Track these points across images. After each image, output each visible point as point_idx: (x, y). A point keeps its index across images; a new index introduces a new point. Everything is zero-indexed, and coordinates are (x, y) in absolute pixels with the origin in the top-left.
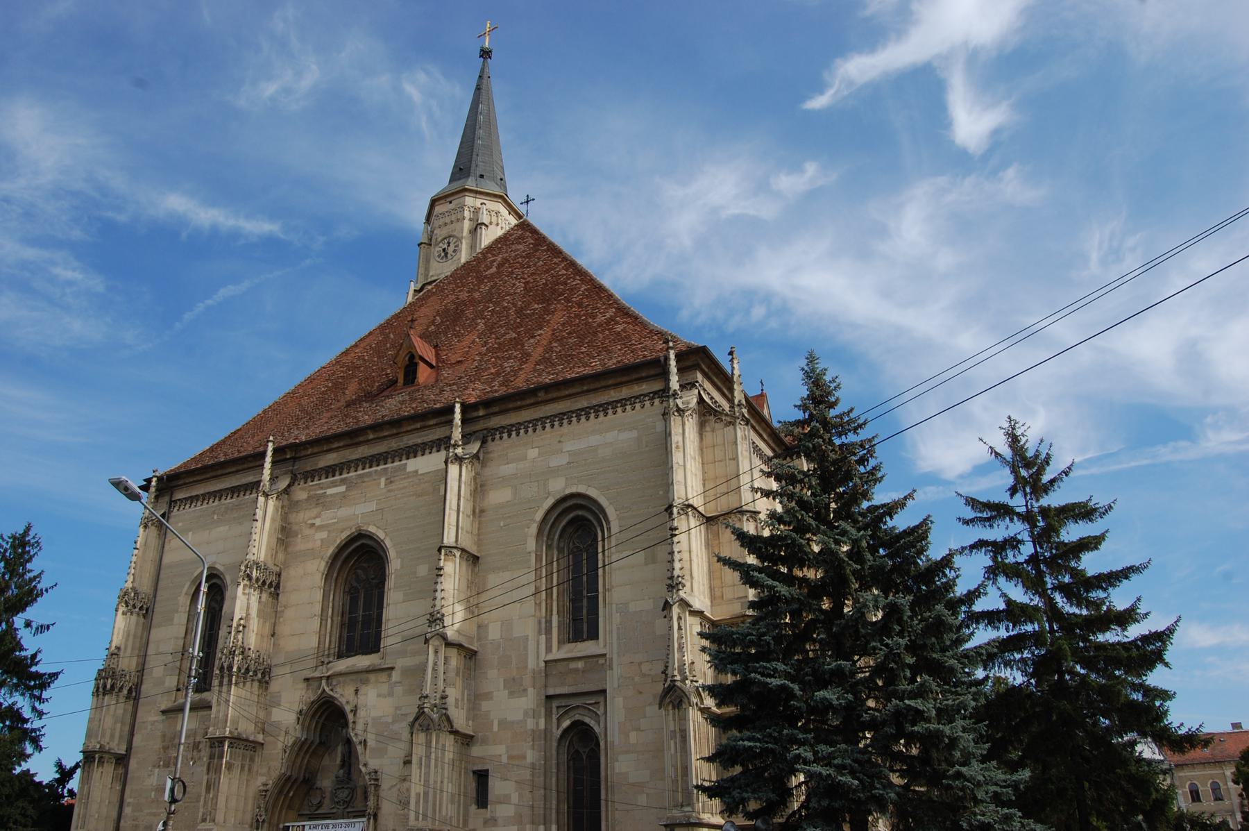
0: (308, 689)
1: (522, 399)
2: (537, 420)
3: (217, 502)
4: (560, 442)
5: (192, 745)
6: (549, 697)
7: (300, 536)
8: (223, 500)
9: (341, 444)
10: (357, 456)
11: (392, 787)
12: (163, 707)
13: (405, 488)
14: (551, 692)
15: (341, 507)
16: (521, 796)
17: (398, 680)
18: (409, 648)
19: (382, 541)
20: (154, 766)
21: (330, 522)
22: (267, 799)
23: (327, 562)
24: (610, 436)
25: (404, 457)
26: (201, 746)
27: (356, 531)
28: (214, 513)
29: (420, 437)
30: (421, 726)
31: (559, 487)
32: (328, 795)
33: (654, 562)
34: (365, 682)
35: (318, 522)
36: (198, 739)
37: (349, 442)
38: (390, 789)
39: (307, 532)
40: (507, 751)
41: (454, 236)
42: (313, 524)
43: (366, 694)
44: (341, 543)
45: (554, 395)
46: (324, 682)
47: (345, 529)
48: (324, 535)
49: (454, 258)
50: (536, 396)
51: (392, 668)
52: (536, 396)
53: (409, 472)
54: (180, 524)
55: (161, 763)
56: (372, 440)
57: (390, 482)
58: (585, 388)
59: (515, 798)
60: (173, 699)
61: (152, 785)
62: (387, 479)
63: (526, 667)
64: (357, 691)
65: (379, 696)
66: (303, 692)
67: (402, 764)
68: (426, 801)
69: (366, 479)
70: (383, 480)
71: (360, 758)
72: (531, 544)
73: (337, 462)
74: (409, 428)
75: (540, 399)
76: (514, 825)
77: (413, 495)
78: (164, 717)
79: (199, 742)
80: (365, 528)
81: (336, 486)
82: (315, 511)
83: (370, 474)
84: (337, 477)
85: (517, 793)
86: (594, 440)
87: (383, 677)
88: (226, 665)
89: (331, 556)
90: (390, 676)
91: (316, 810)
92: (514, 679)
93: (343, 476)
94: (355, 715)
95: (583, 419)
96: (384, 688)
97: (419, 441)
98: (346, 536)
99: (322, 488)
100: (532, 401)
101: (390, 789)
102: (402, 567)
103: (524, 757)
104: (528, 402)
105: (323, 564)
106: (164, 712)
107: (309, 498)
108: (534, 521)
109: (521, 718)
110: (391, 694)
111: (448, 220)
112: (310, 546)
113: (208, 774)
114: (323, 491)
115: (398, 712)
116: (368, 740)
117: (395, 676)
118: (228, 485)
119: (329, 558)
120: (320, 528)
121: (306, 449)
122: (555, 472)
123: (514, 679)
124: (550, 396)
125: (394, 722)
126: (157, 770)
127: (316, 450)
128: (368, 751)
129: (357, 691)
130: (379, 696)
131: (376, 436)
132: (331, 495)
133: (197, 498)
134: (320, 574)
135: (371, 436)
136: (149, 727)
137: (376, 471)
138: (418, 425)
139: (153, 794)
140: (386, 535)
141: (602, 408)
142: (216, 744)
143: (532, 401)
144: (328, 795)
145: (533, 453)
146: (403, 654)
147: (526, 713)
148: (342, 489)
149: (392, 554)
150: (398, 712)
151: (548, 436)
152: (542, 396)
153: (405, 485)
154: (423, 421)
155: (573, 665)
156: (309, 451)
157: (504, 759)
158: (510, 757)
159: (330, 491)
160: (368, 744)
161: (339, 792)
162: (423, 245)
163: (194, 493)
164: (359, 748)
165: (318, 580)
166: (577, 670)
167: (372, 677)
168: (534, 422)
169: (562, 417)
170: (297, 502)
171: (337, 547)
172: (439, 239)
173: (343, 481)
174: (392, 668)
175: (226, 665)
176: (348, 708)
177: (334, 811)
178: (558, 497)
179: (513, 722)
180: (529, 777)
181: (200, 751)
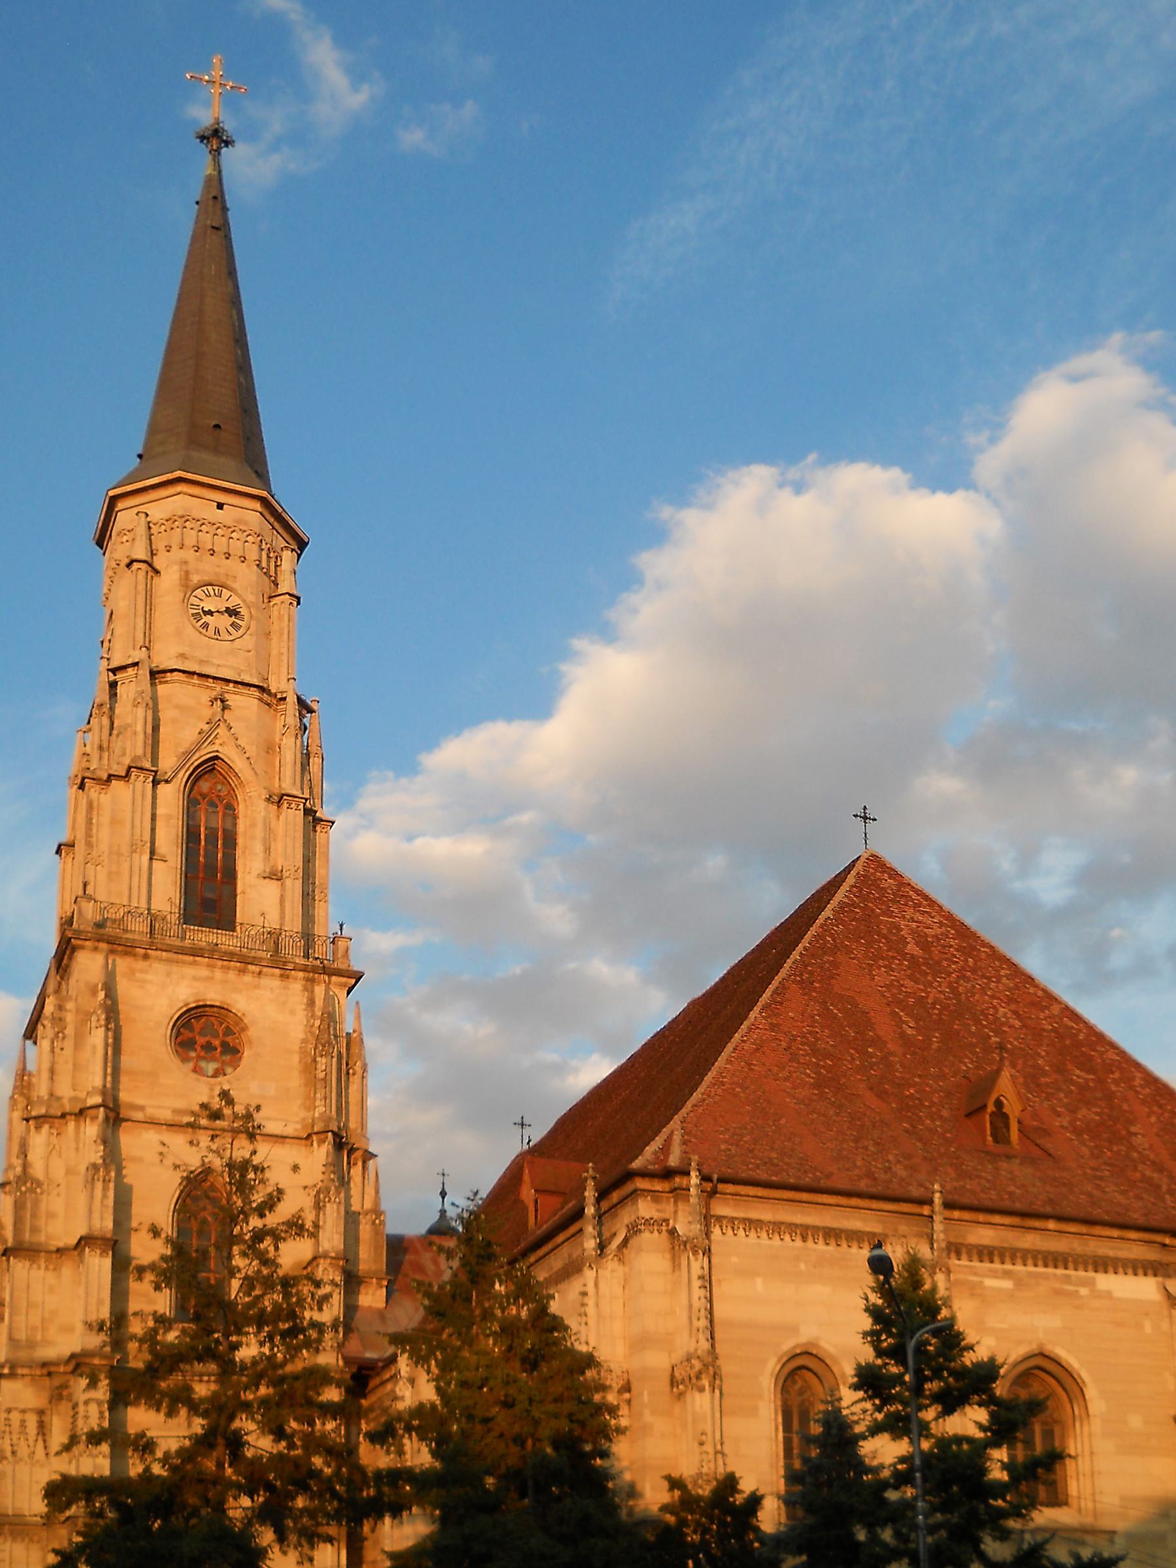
8: (810, 1243)
29: (1112, 1248)
54: (734, 1259)
73: (995, 1243)
81: (996, 1277)
97: (1111, 1253)
99: (975, 1274)
111: (221, 544)
127: (967, 1215)
137: (1055, 1275)
148: (1007, 1284)
149: (1091, 1392)
159: (990, 1282)
163: (754, 1215)
172: (195, 579)
173: (1007, 1274)
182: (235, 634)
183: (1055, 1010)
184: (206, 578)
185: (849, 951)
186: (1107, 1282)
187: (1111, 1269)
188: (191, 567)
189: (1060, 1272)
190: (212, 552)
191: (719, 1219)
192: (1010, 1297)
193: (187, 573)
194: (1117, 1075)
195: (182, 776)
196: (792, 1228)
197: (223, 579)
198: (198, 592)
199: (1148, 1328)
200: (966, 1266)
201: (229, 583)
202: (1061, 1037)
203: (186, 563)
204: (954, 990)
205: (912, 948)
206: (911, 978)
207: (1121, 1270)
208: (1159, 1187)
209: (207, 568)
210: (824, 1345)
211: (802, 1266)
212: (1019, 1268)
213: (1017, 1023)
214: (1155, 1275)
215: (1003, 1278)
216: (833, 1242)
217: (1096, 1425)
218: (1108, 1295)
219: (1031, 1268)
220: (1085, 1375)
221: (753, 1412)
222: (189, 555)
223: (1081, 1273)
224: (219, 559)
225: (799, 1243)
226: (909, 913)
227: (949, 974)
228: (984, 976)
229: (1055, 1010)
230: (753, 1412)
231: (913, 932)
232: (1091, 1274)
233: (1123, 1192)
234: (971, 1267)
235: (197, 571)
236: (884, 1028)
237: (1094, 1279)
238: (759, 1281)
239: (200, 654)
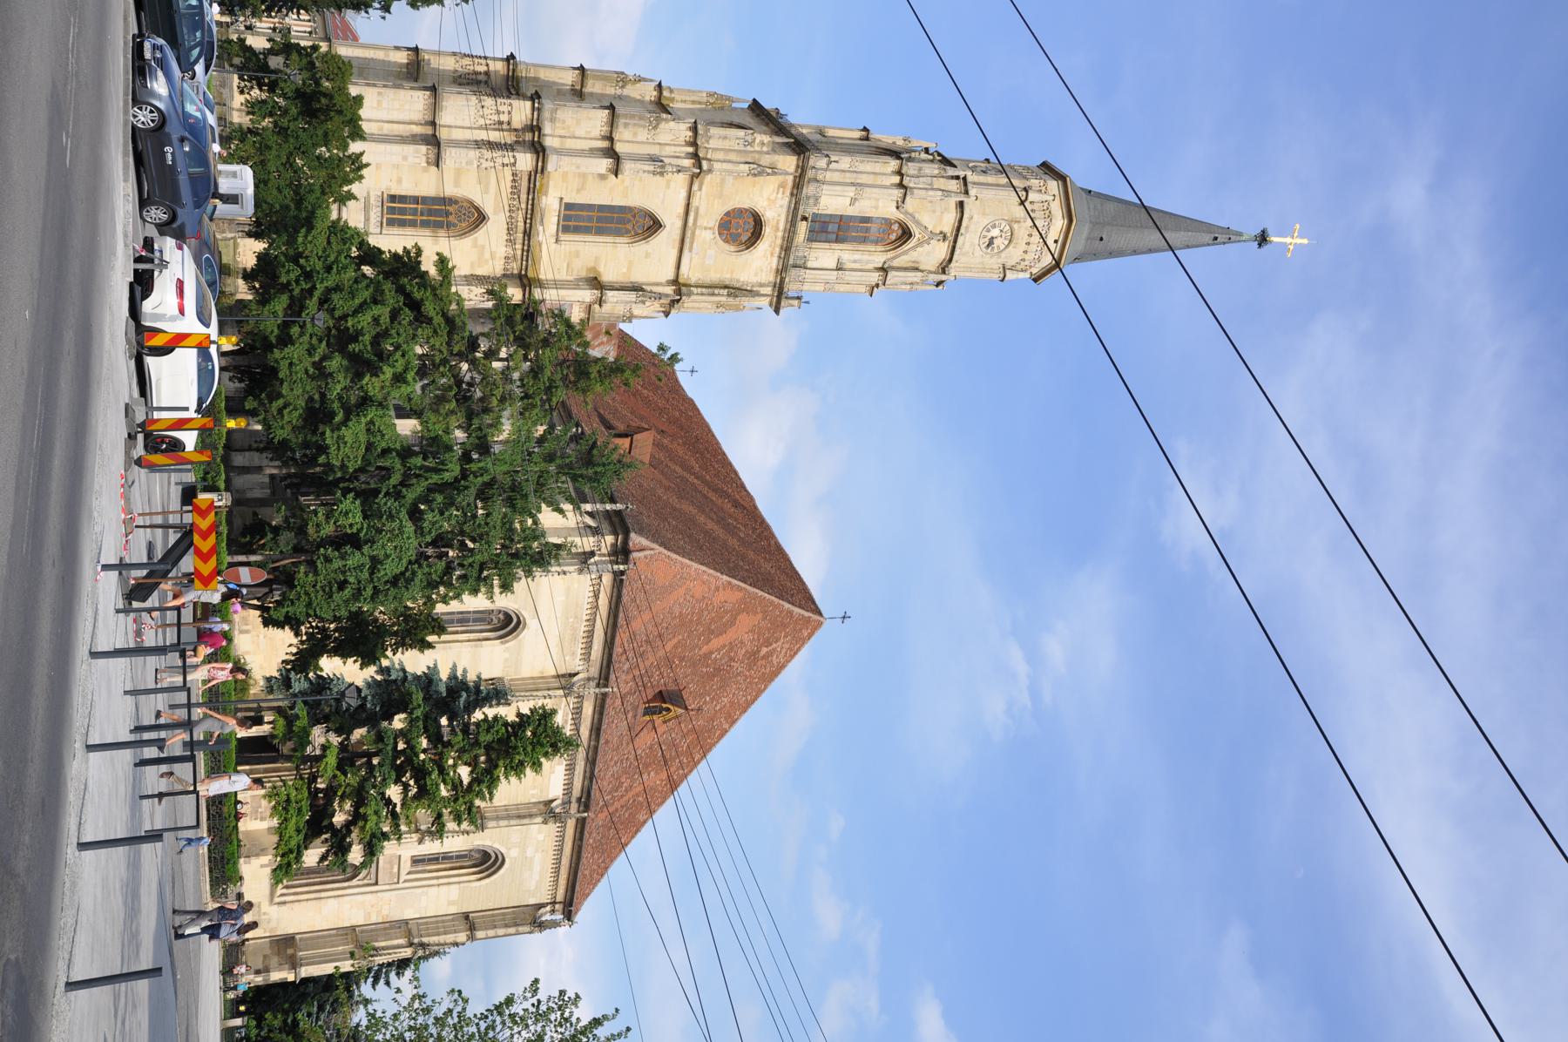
24: (536, 877)
31: (511, 855)
33: (449, 905)
41: (1007, 246)
73: (583, 716)
86: (537, 867)
97: (576, 773)
133: (596, 596)
141: (557, 871)
155: (396, 867)
166: (392, 868)
169: (560, 850)
172: (1016, 226)
183: (726, 726)
184: (1016, 232)
185: (764, 618)
188: (1022, 224)
193: (1019, 222)
194: (685, 761)
195: (901, 217)
198: (1008, 227)
199: (535, 792)
201: (1012, 245)
202: (710, 731)
204: (738, 674)
205: (764, 650)
206: (747, 651)
208: (616, 791)
210: (526, 630)
211: (571, 620)
213: (718, 708)
216: (585, 635)
224: (1026, 239)
226: (787, 646)
227: (749, 670)
228: (747, 688)
229: (726, 726)
231: (774, 650)
233: (613, 775)
236: (715, 643)
238: (564, 598)
239: (972, 227)
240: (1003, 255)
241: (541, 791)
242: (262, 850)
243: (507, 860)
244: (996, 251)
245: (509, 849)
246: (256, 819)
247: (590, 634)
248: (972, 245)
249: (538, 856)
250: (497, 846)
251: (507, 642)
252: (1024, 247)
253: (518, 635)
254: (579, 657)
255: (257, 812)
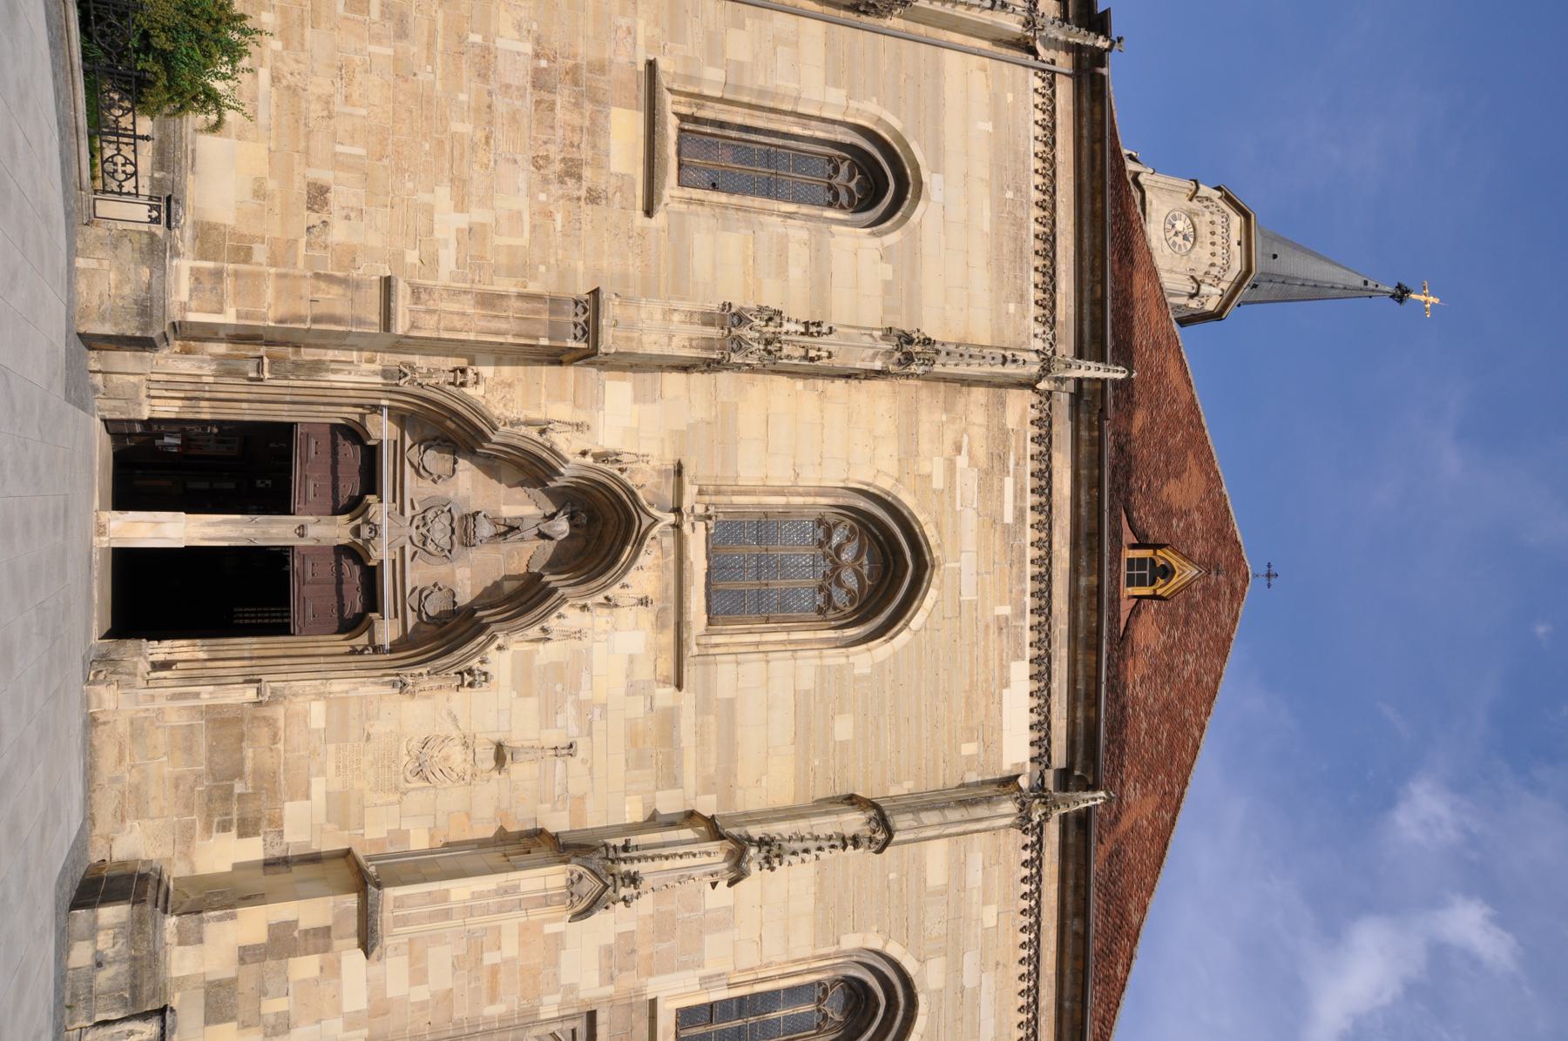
0: (660, 472)
1: (1077, 887)
2: (1038, 916)
3: (1036, 196)
4: (998, 964)
5: (576, 156)
6: (591, 1017)
7: (944, 418)
8: (1037, 212)
9: (1083, 512)
10: (1055, 546)
11: (455, 719)
12: (663, 64)
13: (986, 661)
14: (601, 1018)
15: (979, 515)
16: (423, 1006)
17: (658, 704)
18: (711, 718)
19: (906, 625)
20: (538, 41)
21: (958, 492)
22: (448, 387)
23: (888, 493)
25: (1036, 652)
26: (571, 182)
27: (932, 559)
28: (1018, 190)
30: (580, 877)
31: (929, 978)
32: (441, 489)
34: (660, 625)
35: (962, 461)
36: (587, 173)
37: (1084, 529)
38: (450, 714)
39: (949, 437)
40: (506, 962)
41: (1194, 245)
42: (958, 450)
43: (637, 627)
44: (917, 522)
45: (1069, 950)
46: (671, 518)
47: (938, 526)
48: (938, 482)
49: (1164, 242)
50: (1076, 915)
51: (679, 686)
52: (1076, 915)
53: (1008, 667)
54: (1010, 97)
55: (543, 63)
56: (1077, 580)
57: (1002, 625)
58: (1067, 1004)
59: (421, 993)
60: (675, 87)
61: (497, 34)
62: (1007, 618)
63: (651, 974)
64: (644, 602)
65: (632, 659)
66: (655, 463)
67: (497, 737)
68: (433, 917)
69: (1015, 570)
70: (1005, 610)
71: (517, 636)
72: (851, 942)
73: (1055, 497)
74: (1080, 666)
75: (1068, 922)
76: (369, 1001)
77: (971, 683)
78: (641, 67)
79: (580, 178)
80: (935, 580)
82: (981, 453)
83: (1021, 580)
84: (1031, 499)
85: (427, 996)
87: (667, 666)
88: (745, 332)
89: (899, 501)
90: (665, 682)
91: (412, 464)
92: (633, 951)
93: (1029, 510)
94: (601, 605)
95: (1022, 1001)
96: (644, 672)
97: (1054, 685)
98: (928, 533)
99: (1017, 464)
100: (1070, 908)
101: (450, 714)
102: (856, 679)
103: (493, 1000)
104: (1070, 899)
105: (884, 484)
106: (651, 65)
107: (1004, 433)
108: (886, 942)
109: (566, 978)
110: (632, 688)
111: (1217, 238)
112: (925, 446)
113: (521, 296)
114: (1011, 473)
115: (597, 712)
116: (549, 645)
117: (666, 694)
118: (1060, 226)
119: (895, 498)
120: (951, 466)
121: (1090, 428)
122: (956, 969)
123: (633, 951)
124: (1069, 940)
125: (581, 706)
126: (528, 48)
127: (1084, 449)
128: (528, 647)
129: (644, 602)
130: (632, 659)
131: (1082, 593)
132: (1001, 489)
133: (1051, 143)
134: (870, 481)
135: (1083, 581)
136: (624, 22)
137: (1024, 591)
138: (1081, 686)
139: (476, 38)
140: (916, 633)
142: (581, 319)
143: (1070, 908)
144: (441, 489)
145: (990, 916)
146: (703, 707)
147: (572, 988)
148: (1009, 518)
149: (881, 650)
150: (597, 712)
151: (1011, 942)
152: (1074, 925)
153: (991, 663)
154: (1087, 696)
156: (1084, 434)
157: (490, 958)
158: (494, 970)
159: (1009, 482)
160: (540, 646)
161: (445, 519)
162: (1194, 187)
164: (534, 631)
165: (862, 476)
167: (669, 637)
168: (1036, 912)
170: (1003, 404)
171: (911, 513)
172: (1196, 220)
173: (1020, 515)
174: (679, 686)
175: (745, 332)
176: (614, 591)
177: (408, 512)
178: (916, 982)
179: (556, 964)
180: (456, 1016)
181: (562, 182)
182: (1171, 242)
184: (1198, 227)
186: (1021, 671)
187: (1035, 686)
189: (1028, 598)
190: (1213, 233)
191: (1052, 84)
192: (995, 520)
196: (1050, 190)
197: (1199, 239)
198: (1188, 220)
199: (969, 749)
200: (1025, 449)
201: (1198, 244)
203: (1203, 215)
207: (1035, 702)
209: (1204, 230)
210: (921, 204)
212: (1030, 535)
214: (1032, 760)
215: (1015, 507)
217: (835, 658)
218: (1006, 684)
219: (1031, 553)
220: (919, 619)
221: (832, 80)
222: (1208, 217)
223: (1028, 636)
225: (1036, 196)
230: (832, 80)
232: (1029, 652)
234: (1025, 458)
235: (1200, 222)
237: (1023, 659)
238: (989, 127)
240: (1192, 256)
241: (986, 747)
242: (249, 898)
243: (922, 1000)
244: (1184, 250)
245: (922, 961)
246: (224, 827)
247: (1049, 239)
248: (1159, 239)
249: (989, 981)
250: (894, 950)
251: (886, 233)
252: (1210, 248)
253: (906, 218)
254: (1034, 311)
255: (227, 795)
